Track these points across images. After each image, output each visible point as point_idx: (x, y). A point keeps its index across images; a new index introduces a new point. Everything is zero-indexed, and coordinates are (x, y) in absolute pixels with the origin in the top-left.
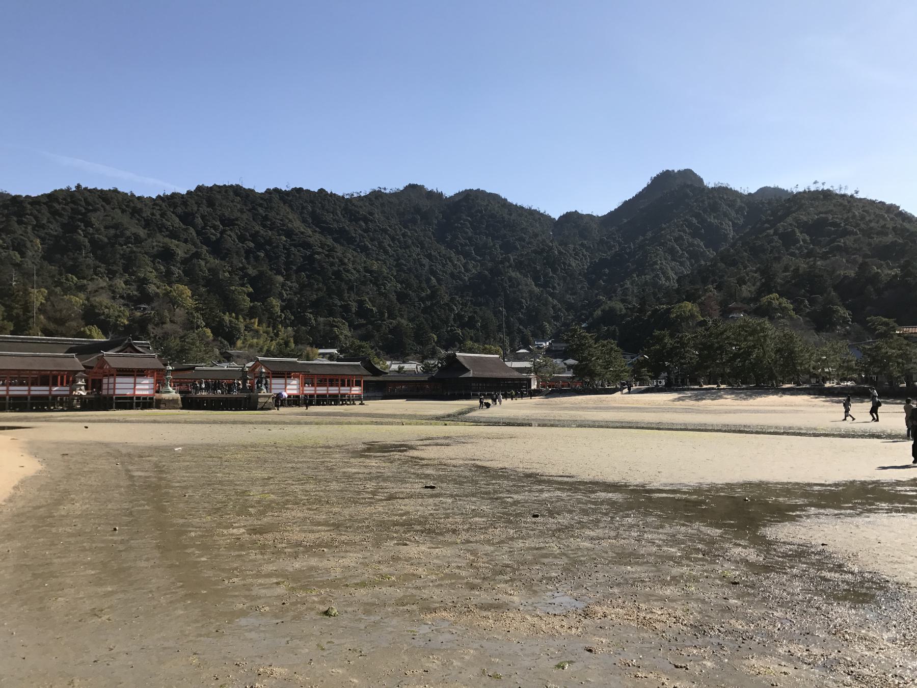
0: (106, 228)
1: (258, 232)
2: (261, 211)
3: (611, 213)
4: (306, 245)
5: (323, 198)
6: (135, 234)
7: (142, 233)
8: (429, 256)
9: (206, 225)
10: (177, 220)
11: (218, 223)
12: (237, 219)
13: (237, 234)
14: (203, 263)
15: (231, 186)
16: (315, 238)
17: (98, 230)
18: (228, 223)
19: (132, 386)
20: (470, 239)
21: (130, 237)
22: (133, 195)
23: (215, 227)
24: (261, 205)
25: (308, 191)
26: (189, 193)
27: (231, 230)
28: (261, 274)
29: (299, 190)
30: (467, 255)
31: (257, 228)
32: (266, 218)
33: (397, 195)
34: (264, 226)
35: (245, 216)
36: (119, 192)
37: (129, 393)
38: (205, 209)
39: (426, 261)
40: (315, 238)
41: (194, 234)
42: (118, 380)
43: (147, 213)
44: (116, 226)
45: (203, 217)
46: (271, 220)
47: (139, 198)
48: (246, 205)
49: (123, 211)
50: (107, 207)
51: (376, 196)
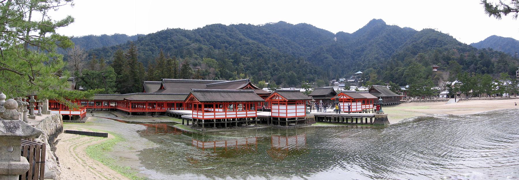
3: (354, 33)
4: (248, 44)
5: (250, 27)
8: (292, 48)
16: (251, 41)
18: (217, 37)
19: (295, 111)
20: (305, 41)
23: (214, 39)
26: (204, 27)
28: (236, 55)
30: (304, 47)
32: (230, 35)
33: (276, 24)
37: (294, 115)
39: (291, 49)
40: (251, 41)
42: (289, 107)
45: (209, 35)
51: (268, 26)
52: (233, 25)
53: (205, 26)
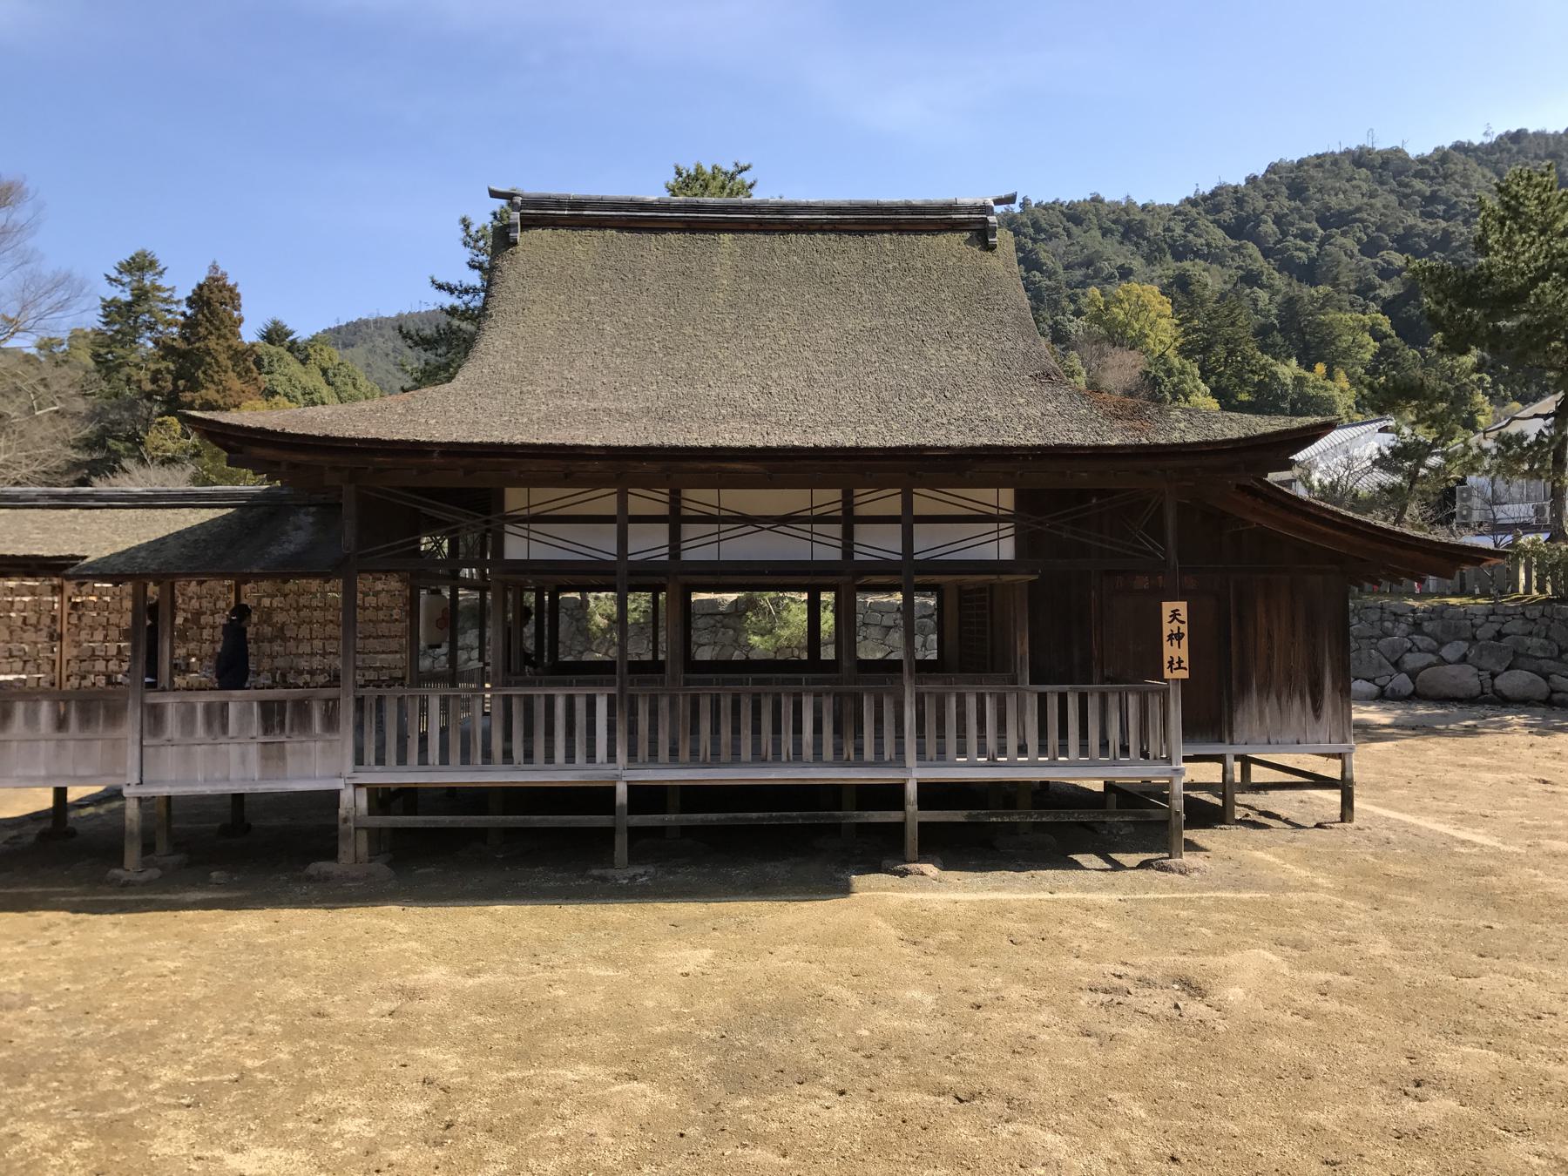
0: (1066, 268)
1: (1412, 227)
2: (1418, 184)
6: (1122, 266)
7: (1137, 264)
9: (1284, 234)
10: (1220, 233)
11: (1314, 225)
12: (1359, 210)
13: (1359, 241)
14: (1263, 295)
15: (1348, 152)
17: (1050, 275)
21: (1111, 276)
22: (1131, 203)
23: (1306, 236)
24: (1420, 175)
25: (1540, 136)
26: (1252, 180)
27: (1344, 234)
29: (1518, 137)
31: (1410, 221)
32: (1433, 198)
34: (1427, 215)
35: (1378, 203)
36: (1102, 201)
38: (1283, 203)
41: (1257, 254)
43: (1156, 230)
44: (1088, 263)
45: (1278, 220)
46: (1445, 201)
47: (1144, 207)
48: (1382, 183)
49: (1105, 232)
50: (1075, 230)
52: (1459, 147)
53: (1260, 171)
